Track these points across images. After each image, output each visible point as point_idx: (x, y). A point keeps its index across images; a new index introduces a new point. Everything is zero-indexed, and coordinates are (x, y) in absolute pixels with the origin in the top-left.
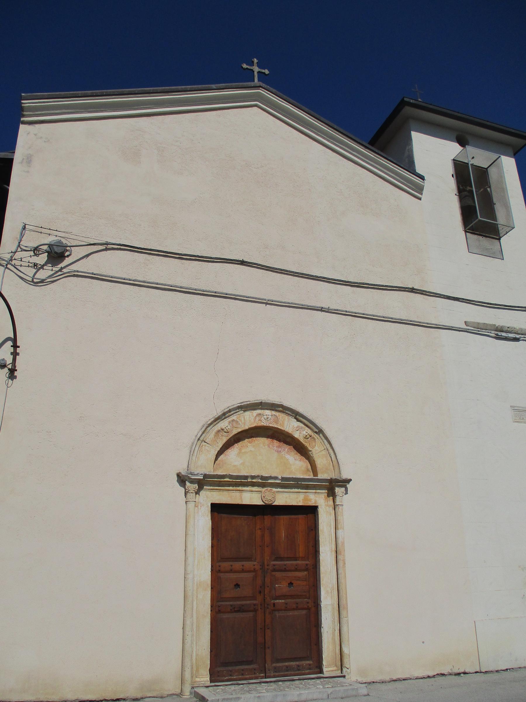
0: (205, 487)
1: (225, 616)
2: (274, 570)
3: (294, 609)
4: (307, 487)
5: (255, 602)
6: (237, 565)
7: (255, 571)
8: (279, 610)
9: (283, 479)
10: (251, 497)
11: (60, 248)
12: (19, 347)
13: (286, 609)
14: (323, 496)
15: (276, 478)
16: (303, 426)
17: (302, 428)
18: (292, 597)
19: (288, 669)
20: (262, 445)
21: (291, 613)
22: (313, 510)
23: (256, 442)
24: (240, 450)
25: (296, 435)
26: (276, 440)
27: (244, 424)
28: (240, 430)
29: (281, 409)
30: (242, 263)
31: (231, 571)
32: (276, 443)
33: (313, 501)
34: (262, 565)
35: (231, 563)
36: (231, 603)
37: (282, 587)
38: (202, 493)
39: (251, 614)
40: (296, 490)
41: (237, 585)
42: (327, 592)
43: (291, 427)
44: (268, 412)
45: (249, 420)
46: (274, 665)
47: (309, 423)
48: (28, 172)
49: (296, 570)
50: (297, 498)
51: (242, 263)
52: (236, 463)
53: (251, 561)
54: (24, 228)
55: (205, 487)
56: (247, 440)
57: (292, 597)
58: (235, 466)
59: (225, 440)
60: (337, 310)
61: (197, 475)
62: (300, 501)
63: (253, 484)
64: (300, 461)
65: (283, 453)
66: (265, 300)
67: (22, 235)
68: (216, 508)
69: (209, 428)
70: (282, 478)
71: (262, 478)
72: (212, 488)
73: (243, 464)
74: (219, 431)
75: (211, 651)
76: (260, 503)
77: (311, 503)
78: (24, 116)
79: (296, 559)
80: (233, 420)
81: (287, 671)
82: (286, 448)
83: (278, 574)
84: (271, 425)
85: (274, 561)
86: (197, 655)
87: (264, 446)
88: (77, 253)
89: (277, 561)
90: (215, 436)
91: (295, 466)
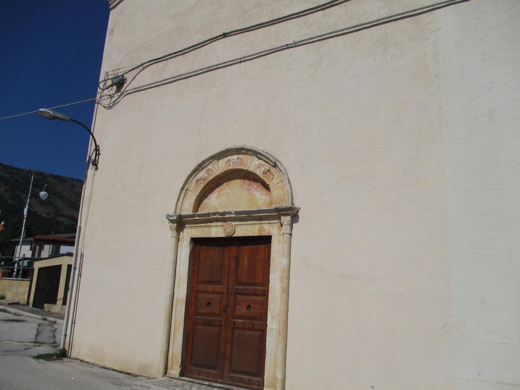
0: (186, 226)
1: (199, 327)
2: (237, 293)
3: (250, 329)
4: (261, 219)
5: (220, 319)
6: (210, 288)
7: (222, 293)
8: (238, 328)
9: (236, 213)
10: (216, 231)
11: (116, 80)
13: (243, 329)
14: (277, 226)
15: (230, 213)
16: (263, 162)
17: (262, 164)
18: (250, 318)
19: (241, 380)
20: (235, 186)
21: (247, 332)
22: (267, 240)
23: (232, 184)
24: (219, 193)
26: (248, 180)
27: (217, 170)
28: (213, 177)
29: (244, 151)
30: (225, 35)
31: (205, 292)
32: (247, 182)
33: (267, 232)
34: (228, 289)
35: (205, 286)
36: (204, 317)
37: (242, 309)
38: (186, 230)
39: (217, 329)
40: (252, 222)
41: (209, 304)
42: (273, 317)
43: (253, 165)
44: (235, 157)
45: (220, 167)
46: (231, 374)
49: (254, 295)
50: (253, 229)
51: (225, 35)
52: (216, 204)
53: (221, 284)
55: (186, 226)
56: (225, 184)
57: (250, 318)
58: (214, 206)
59: (202, 186)
60: (302, 41)
62: (255, 232)
63: (217, 220)
64: (266, 195)
65: (252, 191)
66: (237, 59)
68: (196, 242)
69: (190, 180)
70: (235, 212)
71: (220, 214)
72: (190, 225)
73: (220, 204)
74: (198, 180)
75: (182, 352)
78: (110, 5)
79: (255, 284)
80: (209, 169)
81: (240, 382)
82: (255, 185)
83: (240, 297)
84: (237, 168)
85: (238, 285)
86: (173, 353)
87: (238, 186)
88: (129, 77)
89: (240, 285)
90: (196, 184)
91: (260, 200)
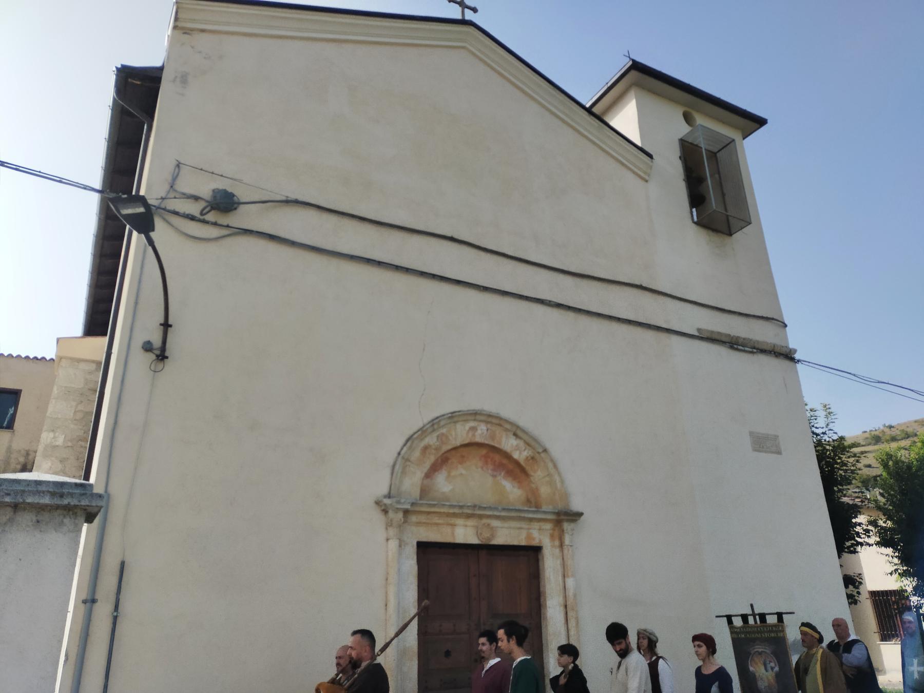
10: (464, 533)
12: (171, 326)
22: (535, 551)
24: (449, 472)
25: (516, 456)
30: (452, 239)
45: (460, 434)
47: (530, 441)
48: (183, 95)
51: (452, 239)
54: (178, 165)
61: (404, 503)
65: (499, 478)
67: (175, 178)
68: (422, 547)
76: (474, 540)
77: (535, 543)
80: (443, 434)
